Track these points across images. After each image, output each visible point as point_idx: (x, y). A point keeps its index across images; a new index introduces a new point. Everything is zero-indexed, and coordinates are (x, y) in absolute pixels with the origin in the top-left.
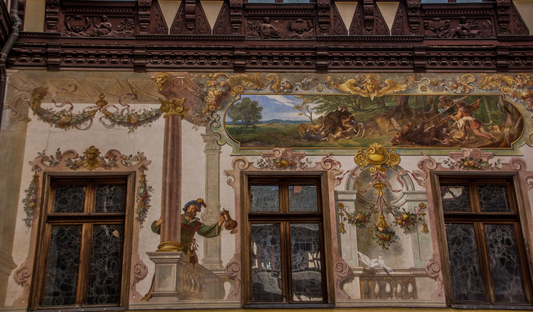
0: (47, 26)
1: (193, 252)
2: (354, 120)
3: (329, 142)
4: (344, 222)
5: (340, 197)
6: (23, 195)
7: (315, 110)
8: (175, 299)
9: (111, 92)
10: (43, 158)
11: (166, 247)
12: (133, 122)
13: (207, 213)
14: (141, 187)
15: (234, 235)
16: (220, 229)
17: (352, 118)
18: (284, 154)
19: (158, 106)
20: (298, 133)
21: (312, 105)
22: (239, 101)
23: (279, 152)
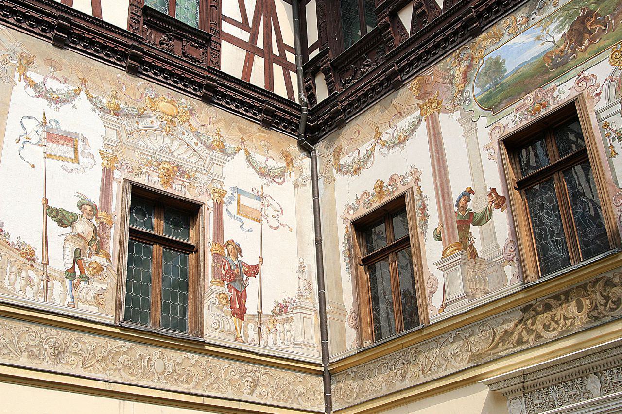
0: (330, 91)
1: (471, 246)
2: (600, 16)
3: (578, 59)
4: (613, 144)
5: (603, 115)
6: (341, 248)
7: (556, 31)
8: (465, 301)
9: (382, 121)
10: (349, 209)
11: (448, 252)
12: (401, 140)
13: (477, 200)
14: (419, 200)
15: (505, 212)
16: (490, 211)
17: (597, 15)
18: (536, 96)
19: (418, 112)
20: (544, 66)
21: (552, 27)
22: (481, 65)
23: (529, 100)
